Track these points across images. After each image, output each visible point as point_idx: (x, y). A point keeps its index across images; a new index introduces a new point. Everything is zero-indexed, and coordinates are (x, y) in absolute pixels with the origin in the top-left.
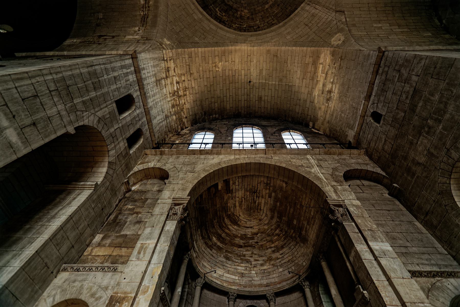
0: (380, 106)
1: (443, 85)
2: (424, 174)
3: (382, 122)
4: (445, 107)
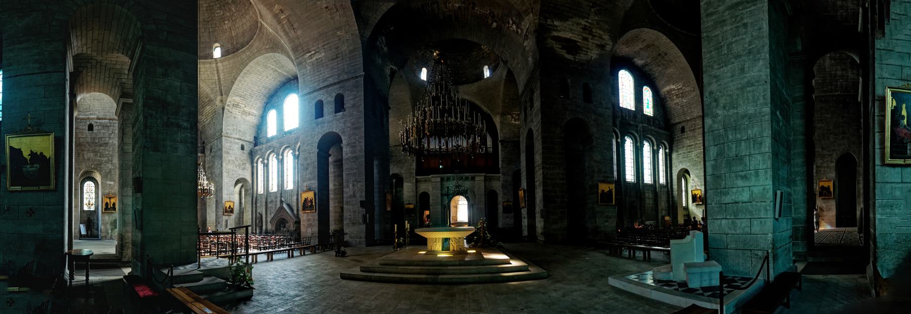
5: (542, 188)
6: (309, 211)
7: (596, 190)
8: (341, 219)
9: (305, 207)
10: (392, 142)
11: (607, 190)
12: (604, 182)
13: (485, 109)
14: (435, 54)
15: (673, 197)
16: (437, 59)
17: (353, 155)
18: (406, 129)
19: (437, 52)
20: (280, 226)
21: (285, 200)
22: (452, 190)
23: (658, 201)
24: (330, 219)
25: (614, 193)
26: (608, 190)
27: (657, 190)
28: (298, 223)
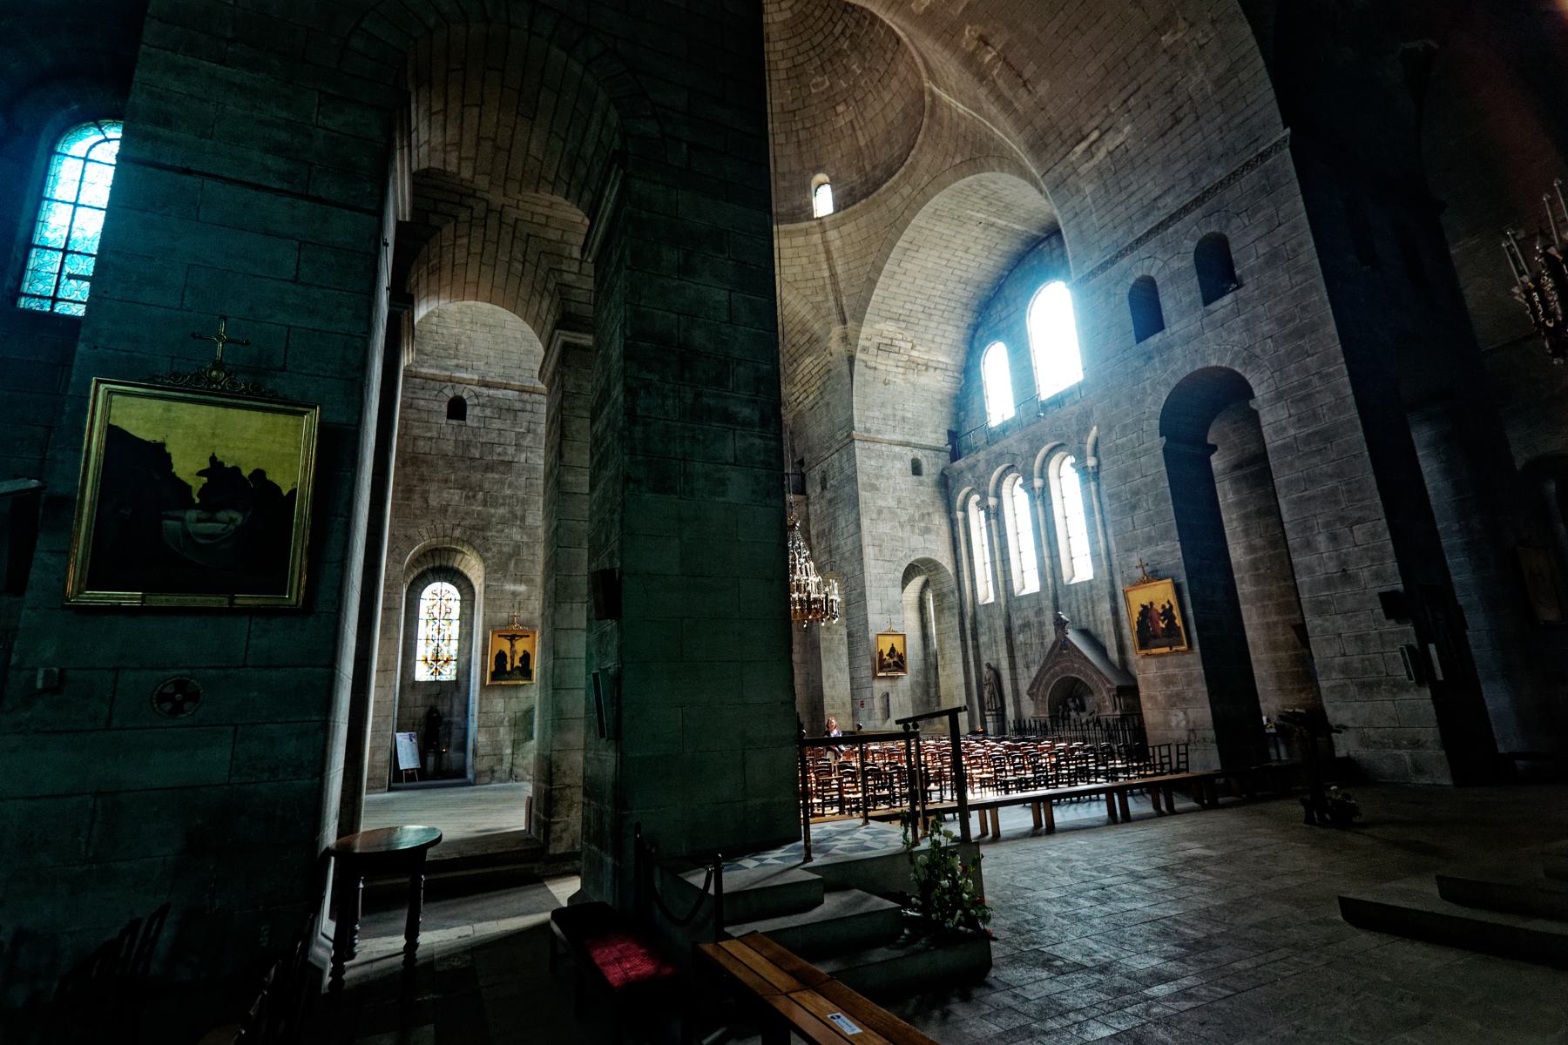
0: (477, 411)
1: (521, 494)
2: (418, 512)
3: (454, 422)
4: (502, 505)
6: (1167, 650)
8: (1302, 671)
9: (1147, 637)
17: (1306, 431)
20: (1066, 705)
21: (1072, 619)
24: (1256, 672)
28: (1129, 691)
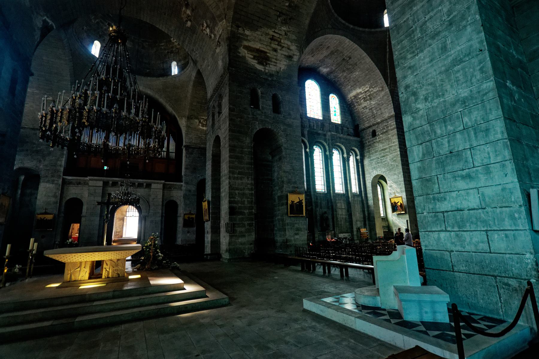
5: (228, 199)
7: (286, 201)
10: (26, 121)
11: (296, 201)
12: (293, 192)
13: (170, 109)
14: (111, 29)
15: (368, 207)
16: (113, 36)
18: (52, 110)
19: (114, 27)
22: (119, 198)
23: (351, 211)
25: (304, 204)
26: (298, 200)
27: (350, 200)
